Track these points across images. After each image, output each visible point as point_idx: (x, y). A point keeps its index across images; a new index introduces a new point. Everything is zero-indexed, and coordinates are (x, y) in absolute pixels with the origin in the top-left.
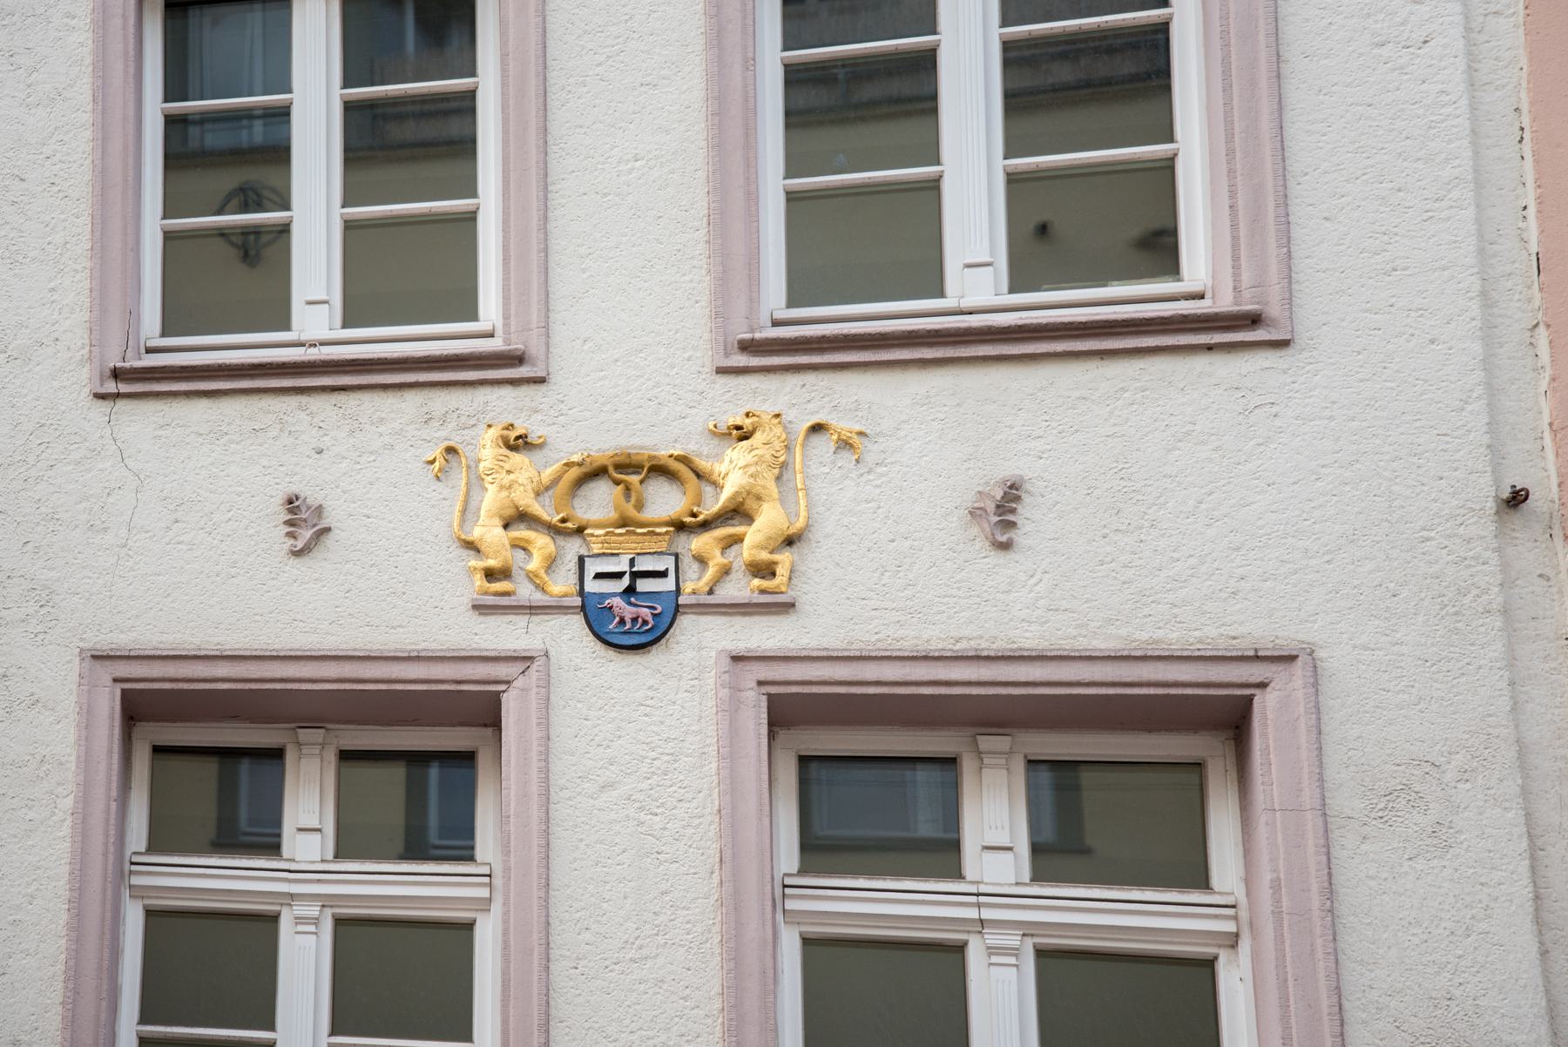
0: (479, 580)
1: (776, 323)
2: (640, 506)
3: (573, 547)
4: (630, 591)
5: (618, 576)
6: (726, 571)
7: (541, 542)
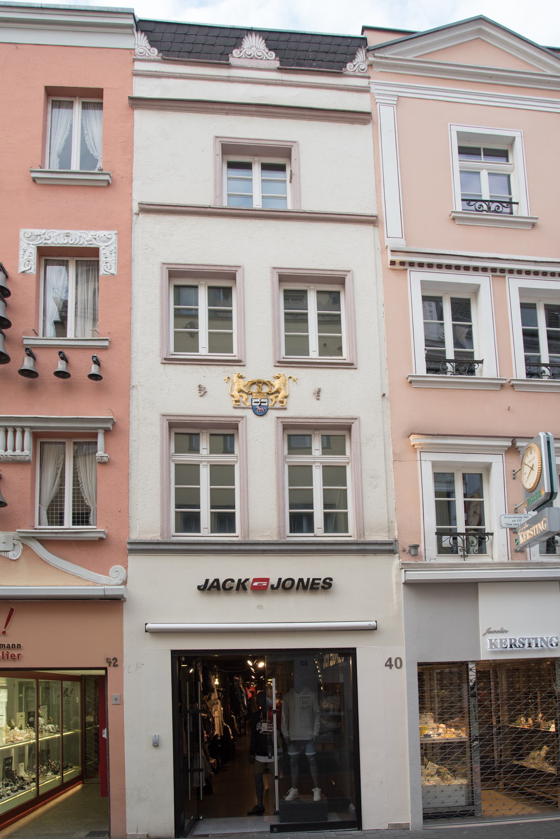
0: (234, 402)
1: (284, 358)
2: (261, 390)
3: (250, 397)
4: (260, 405)
5: (258, 402)
6: (276, 402)
7: (245, 396)
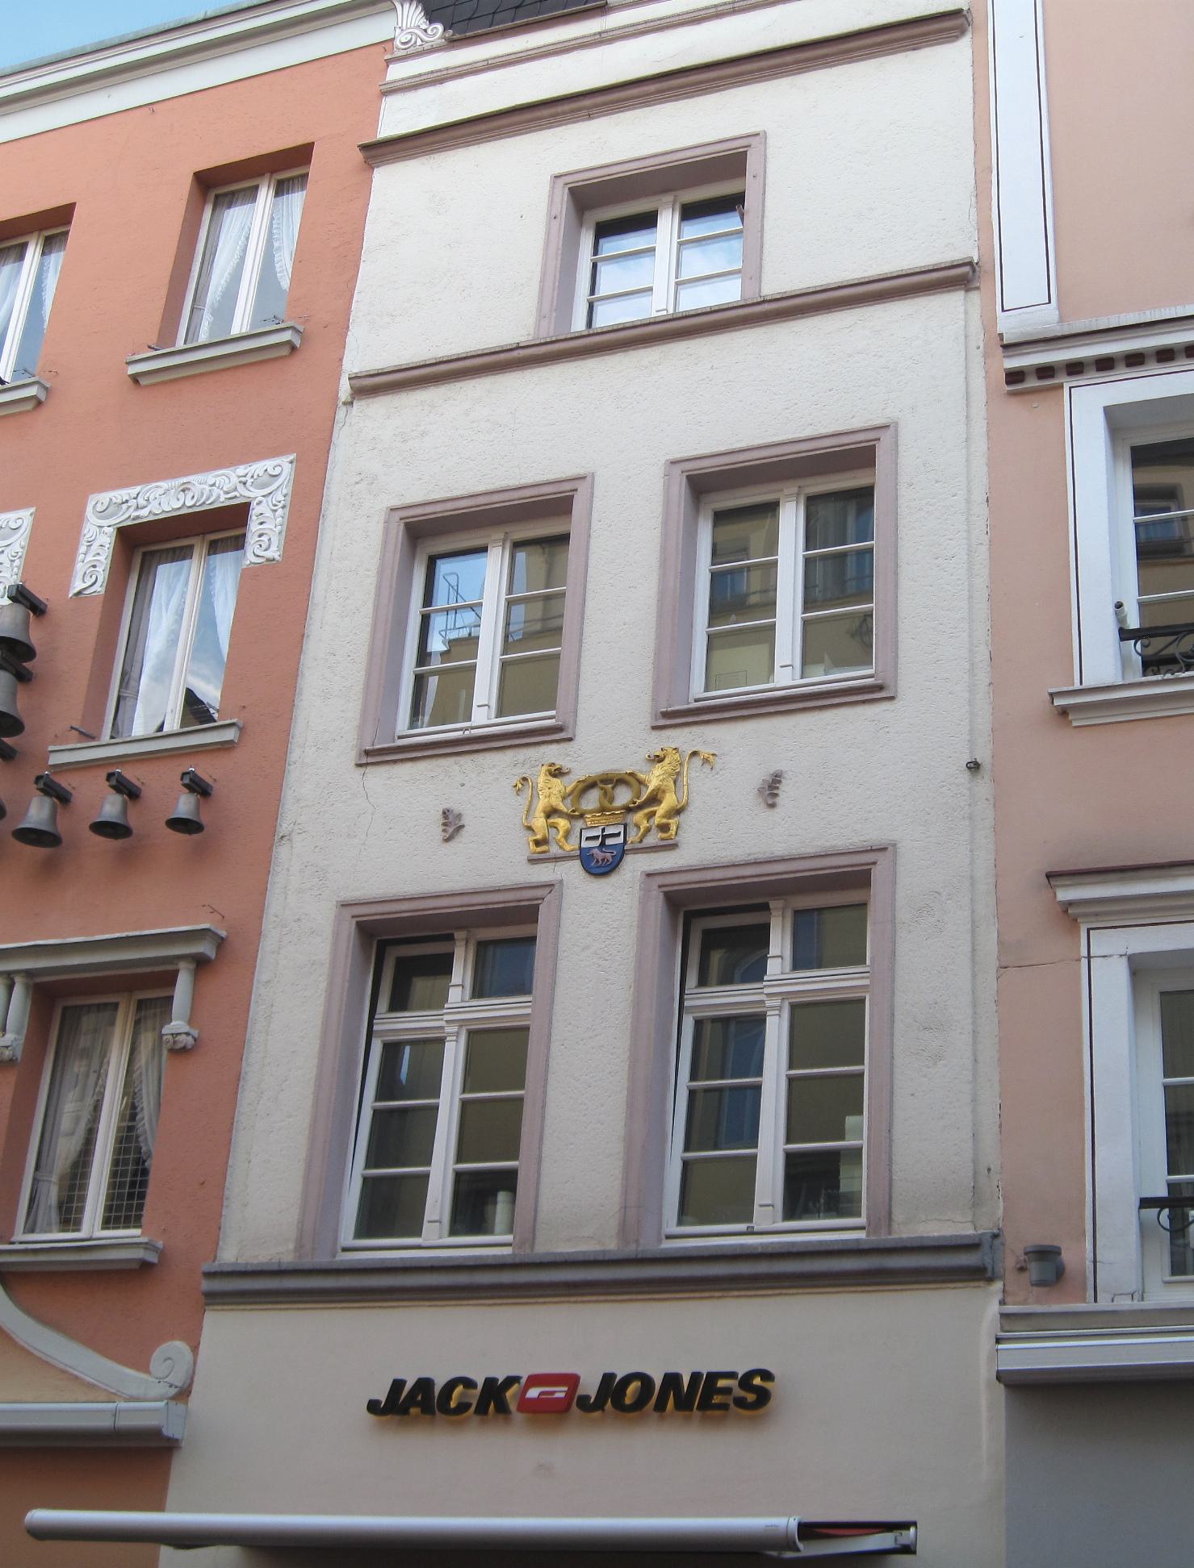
0: (532, 846)
3: (579, 824)
4: (603, 844)
6: (648, 830)
7: (563, 823)
